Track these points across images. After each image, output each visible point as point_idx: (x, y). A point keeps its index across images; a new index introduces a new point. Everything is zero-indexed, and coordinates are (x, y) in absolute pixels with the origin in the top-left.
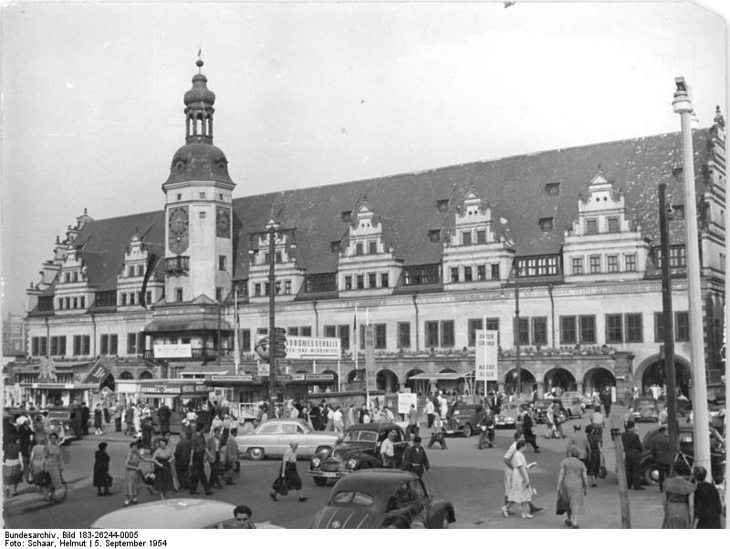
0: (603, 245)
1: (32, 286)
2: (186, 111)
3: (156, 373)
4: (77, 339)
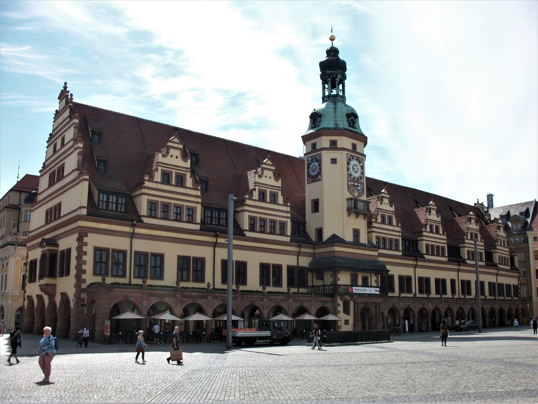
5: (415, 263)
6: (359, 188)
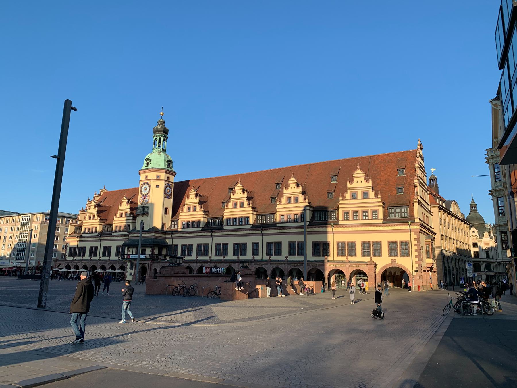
0: (360, 204)
5: (210, 234)
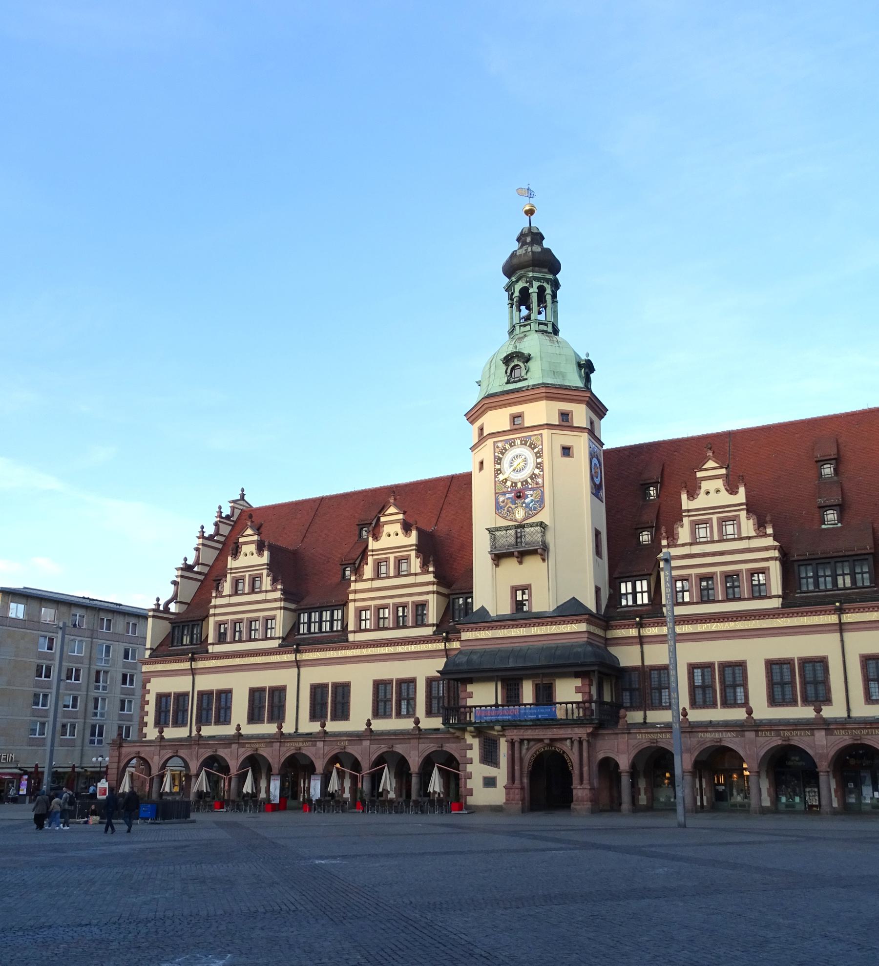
1: (159, 605)
2: (509, 288)
3: (469, 754)
4: (255, 694)
5: (833, 619)
6: (527, 501)
